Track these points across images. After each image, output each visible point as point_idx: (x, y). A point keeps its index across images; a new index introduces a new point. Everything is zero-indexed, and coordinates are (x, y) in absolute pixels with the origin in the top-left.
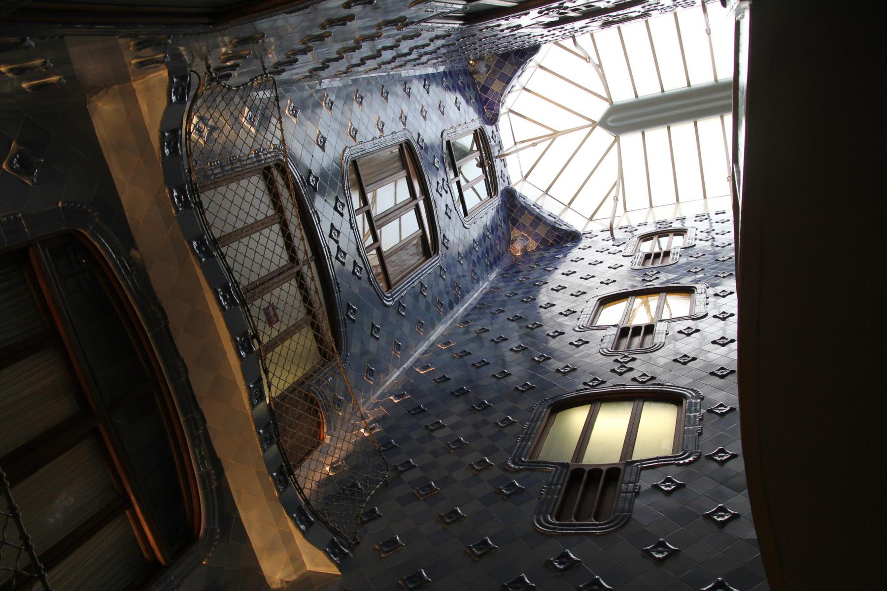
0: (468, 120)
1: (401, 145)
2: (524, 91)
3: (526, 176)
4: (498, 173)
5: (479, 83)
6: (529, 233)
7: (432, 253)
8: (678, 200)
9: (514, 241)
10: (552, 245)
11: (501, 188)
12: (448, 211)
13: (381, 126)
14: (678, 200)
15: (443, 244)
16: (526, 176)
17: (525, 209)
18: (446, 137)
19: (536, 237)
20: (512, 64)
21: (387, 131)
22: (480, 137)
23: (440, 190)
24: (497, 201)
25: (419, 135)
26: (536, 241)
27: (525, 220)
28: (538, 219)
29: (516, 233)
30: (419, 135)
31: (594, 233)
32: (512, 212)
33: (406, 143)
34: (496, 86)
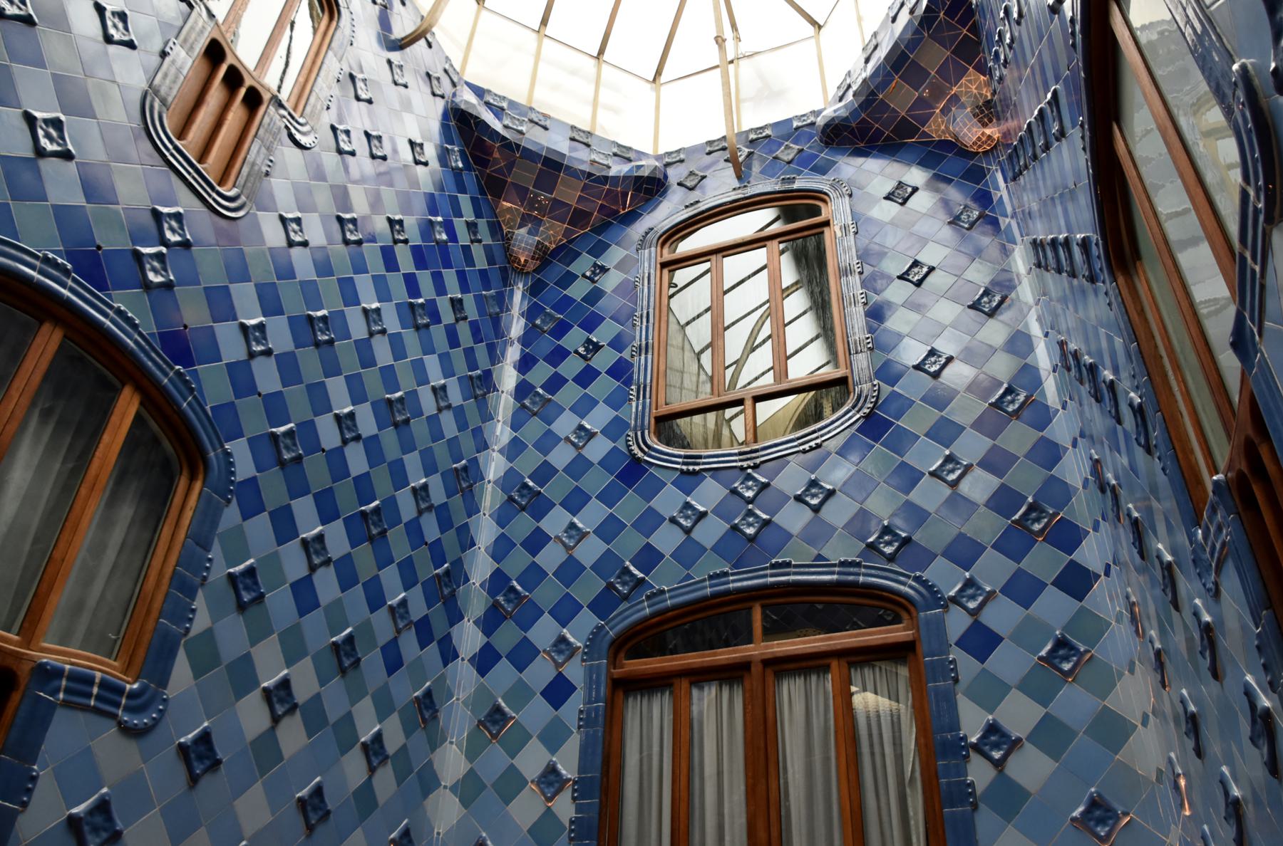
2: (606, 57)
3: (813, 23)
5: (567, 233)
6: (938, 93)
9: (957, 139)
10: (975, 29)
16: (813, 23)
17: (871, 96)
19: (951, 73)
20: (510, 166)
26: (962, 72)
27: (902, 99)
28: (900, 62)
29: (937, 128)
32: (879, 133)
34: (569, 194)
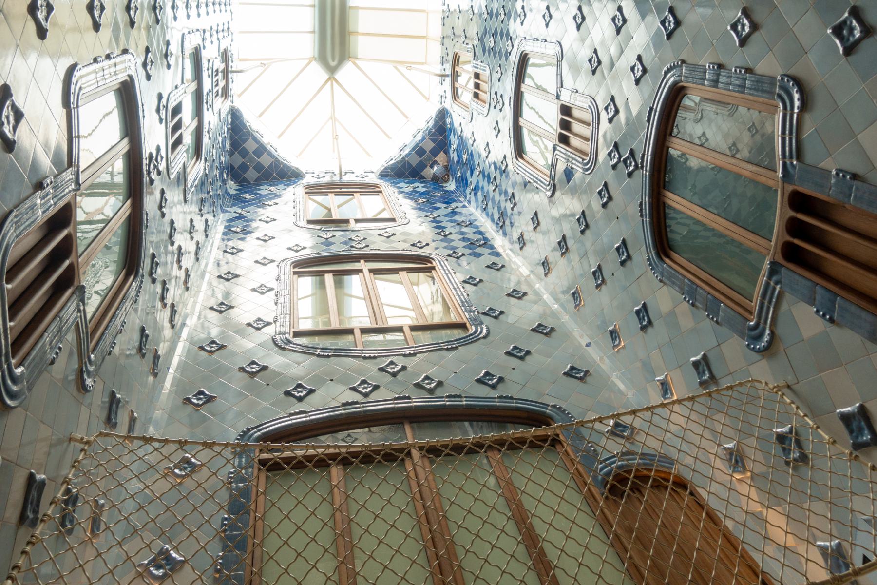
0: (293, 197)
1: (295, 273)
4: (358, 180)
7: (429, 265)
8: (423, 37)
11: (373, 179)
12: (387, 235)
13: (262, 290)
14: (423, 37)
15: (421, 248)
18: (303, 223)
21: (273, 284)
22: (314, 190)
23: (361, 246)
24: (387, 187)
25: (289, 249)
30: (289, 249)
31: (443, 94)
33: (294, 267)
